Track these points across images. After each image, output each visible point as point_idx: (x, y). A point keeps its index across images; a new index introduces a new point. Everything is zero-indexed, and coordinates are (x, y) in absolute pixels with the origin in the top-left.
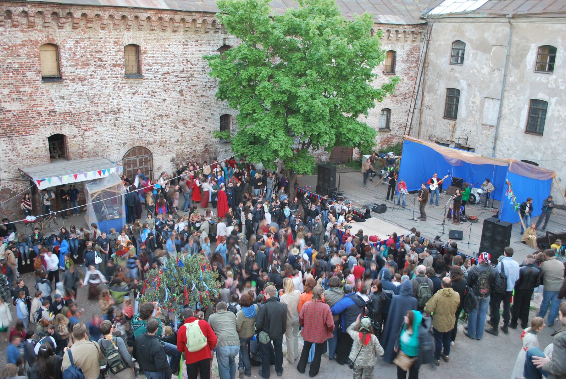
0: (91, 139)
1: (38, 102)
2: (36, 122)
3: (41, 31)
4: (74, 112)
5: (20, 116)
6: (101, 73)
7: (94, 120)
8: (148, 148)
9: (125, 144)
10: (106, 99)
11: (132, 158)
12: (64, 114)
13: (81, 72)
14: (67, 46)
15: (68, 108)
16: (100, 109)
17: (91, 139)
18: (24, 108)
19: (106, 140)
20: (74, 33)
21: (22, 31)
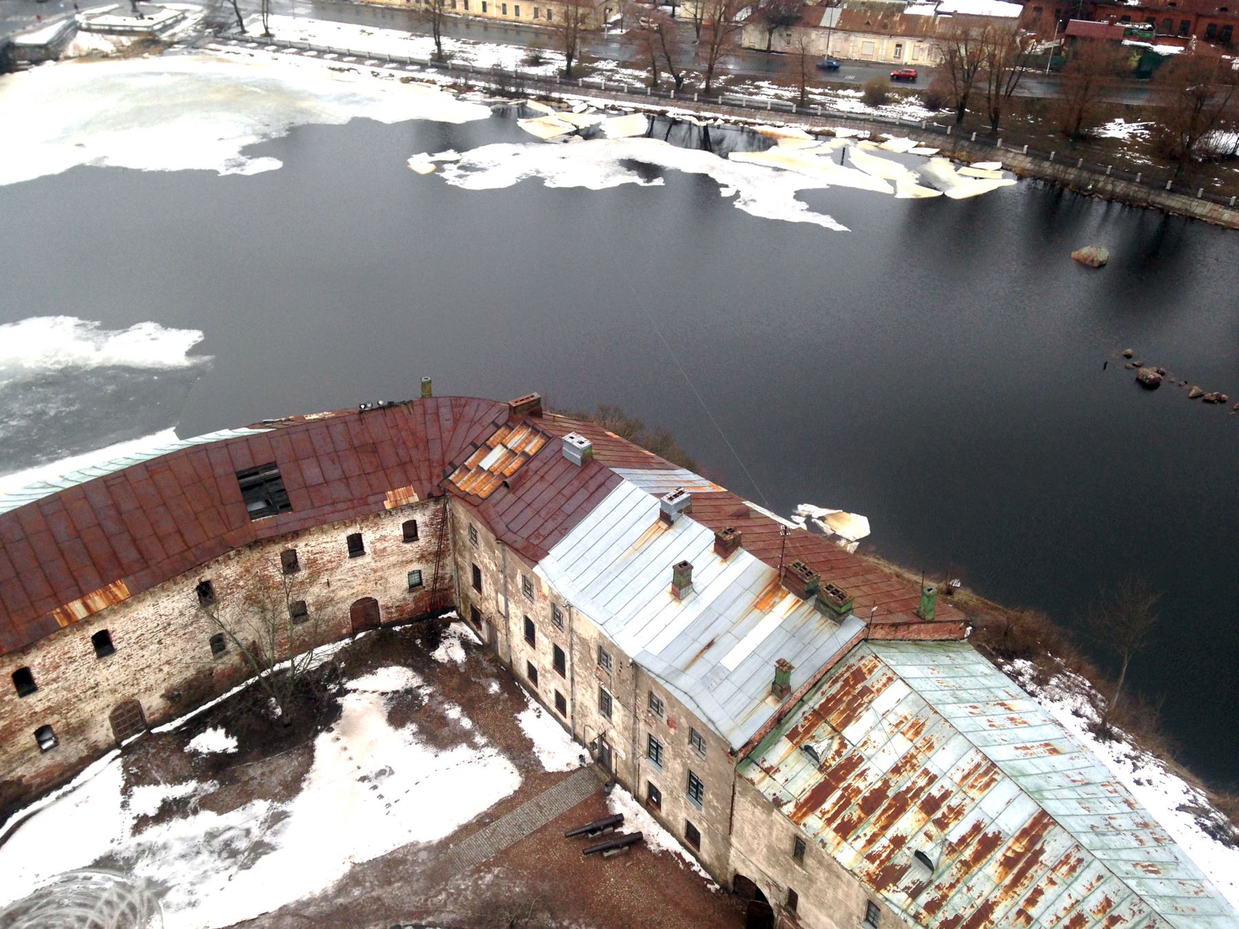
6: (73, 666)
15: (47, 704)
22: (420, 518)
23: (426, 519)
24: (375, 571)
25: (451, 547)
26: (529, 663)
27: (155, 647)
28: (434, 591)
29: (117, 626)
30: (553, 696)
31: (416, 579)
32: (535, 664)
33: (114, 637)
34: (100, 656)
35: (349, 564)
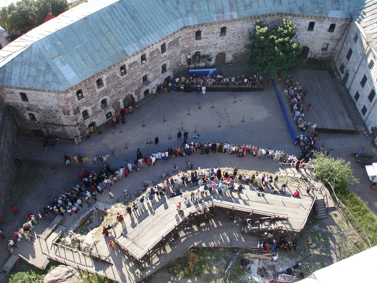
5: (189, 48)
6: (212, 36)
22: (338, 25)
23: (339, 25)
24: (313, 38)
25: (344, 39)
26: (357, 92)
27: (237, 38)
28: (331, 53)
29: (230, 28)
30: (362, 107)
31: (325, 46)
32: (360, 94)
33: (227, 30)
34: (221, 35)
35: (306, 32)
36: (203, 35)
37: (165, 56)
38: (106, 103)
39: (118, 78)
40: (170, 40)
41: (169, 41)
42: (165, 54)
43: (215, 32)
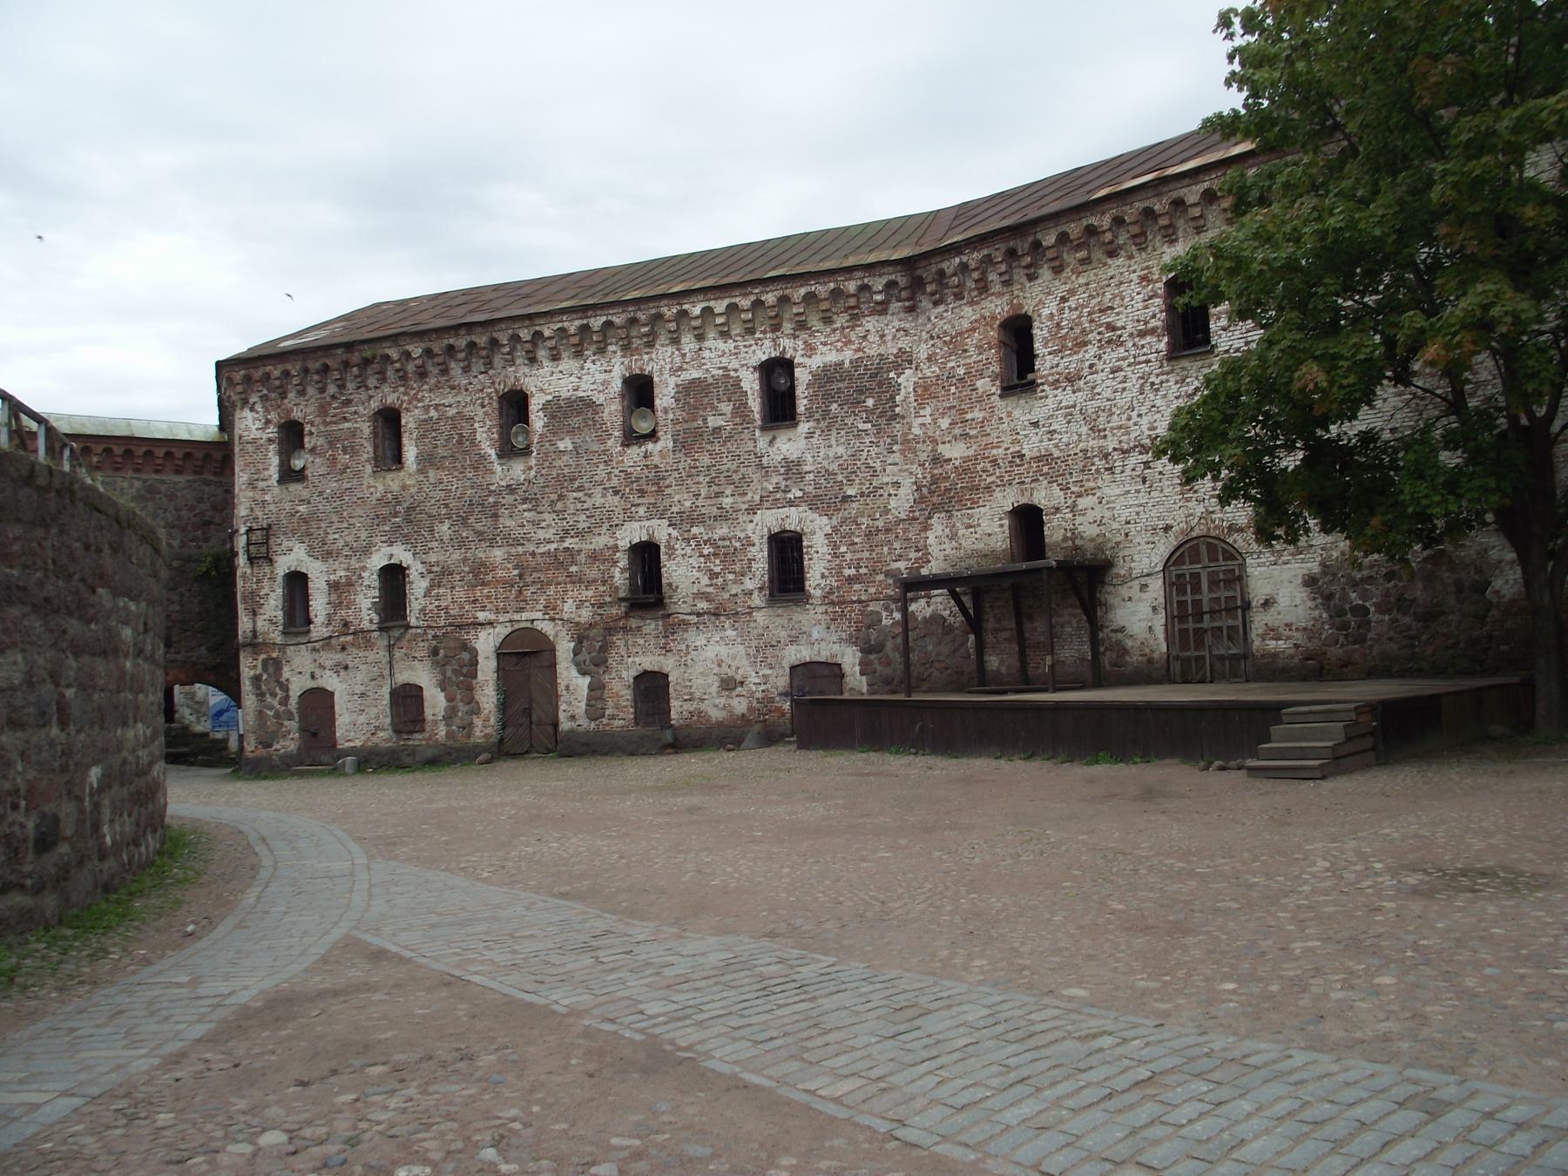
0: (1090, 516)
1: (993, 439)
2: (989, 480)
3: (1001, 294)
4: (1056, 453)
5: (966, 468)
6: (1112, 356)
7: (1098, 471)
8: (1230, 540)
9: (1167, 528)
10: (1124, 417)
11: (1187, 568)
12: (1039, 459)
13: (1069, 363)
14: (1046, 312)
16: (1110, 444)
17: (1090, 516)
18: (971, 452)
19: (1123, 519)
20: (1057, 283)
21: (971, 303)
34: (1173, 355)
36: (1046, 362)
37: (792, 469)
38: (405, 617)
39: (480, 463)
40: (826, 356)
41: (816, 362)
42: (789, 445)
43: (1125, 320)
